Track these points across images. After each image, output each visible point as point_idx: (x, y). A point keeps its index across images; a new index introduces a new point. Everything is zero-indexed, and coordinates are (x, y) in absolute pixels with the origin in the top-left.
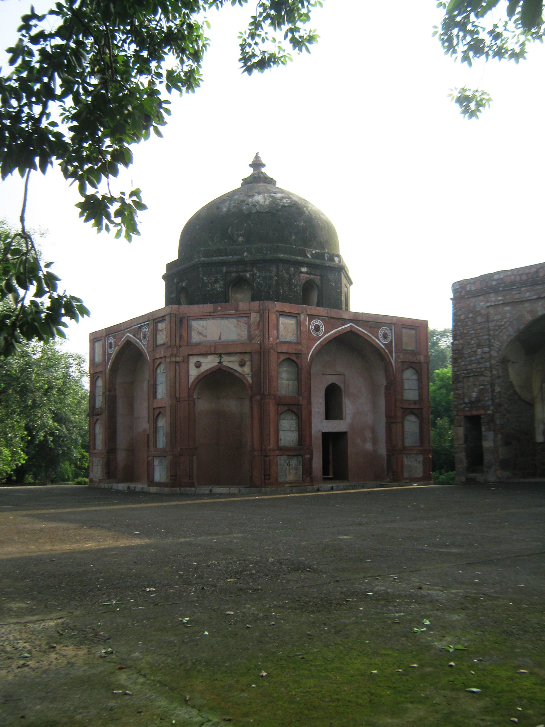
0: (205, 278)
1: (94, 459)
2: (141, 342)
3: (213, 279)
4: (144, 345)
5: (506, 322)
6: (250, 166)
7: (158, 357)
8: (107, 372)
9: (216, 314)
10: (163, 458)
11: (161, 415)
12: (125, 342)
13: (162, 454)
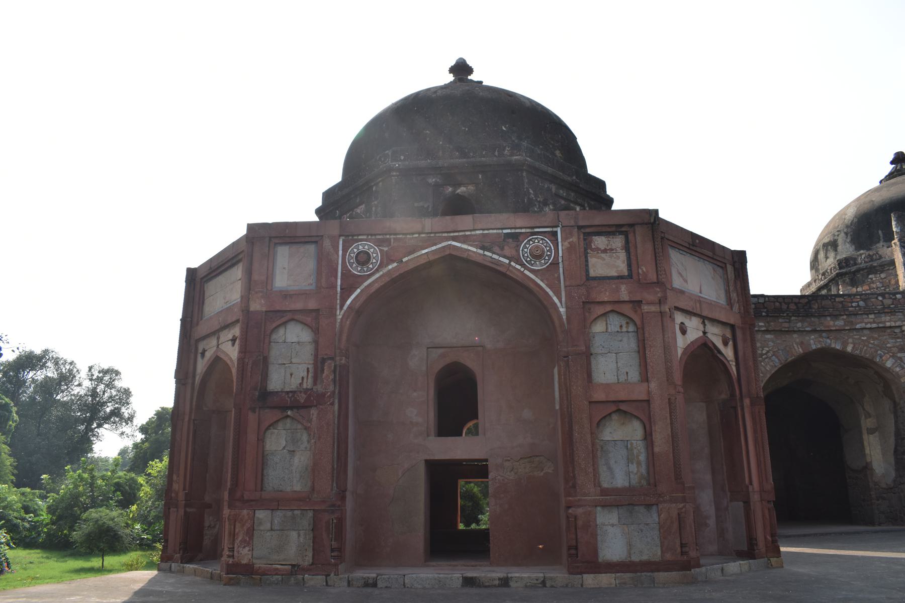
0: (531, 191)
1: (261, 514)
2: (523, 265)
3: (540, 199)
4: (532, 271)
5: (768, 352)
6: (452, 70)
7: (606, 299)
8: (340, 315)
9: (694, 248)
10: (642, 509)
11: (615, 417)
12: (432, 258)
13: (623, 500)
